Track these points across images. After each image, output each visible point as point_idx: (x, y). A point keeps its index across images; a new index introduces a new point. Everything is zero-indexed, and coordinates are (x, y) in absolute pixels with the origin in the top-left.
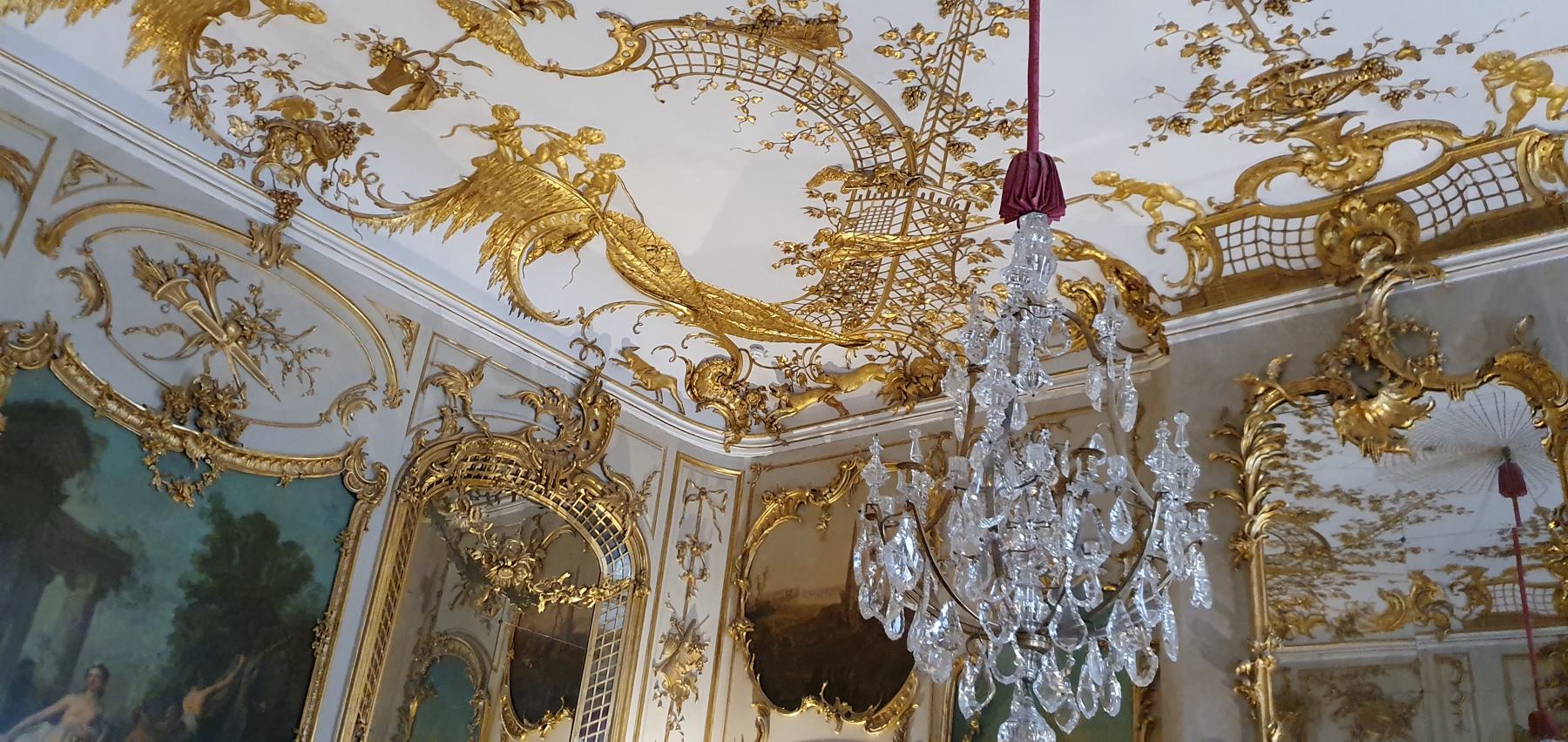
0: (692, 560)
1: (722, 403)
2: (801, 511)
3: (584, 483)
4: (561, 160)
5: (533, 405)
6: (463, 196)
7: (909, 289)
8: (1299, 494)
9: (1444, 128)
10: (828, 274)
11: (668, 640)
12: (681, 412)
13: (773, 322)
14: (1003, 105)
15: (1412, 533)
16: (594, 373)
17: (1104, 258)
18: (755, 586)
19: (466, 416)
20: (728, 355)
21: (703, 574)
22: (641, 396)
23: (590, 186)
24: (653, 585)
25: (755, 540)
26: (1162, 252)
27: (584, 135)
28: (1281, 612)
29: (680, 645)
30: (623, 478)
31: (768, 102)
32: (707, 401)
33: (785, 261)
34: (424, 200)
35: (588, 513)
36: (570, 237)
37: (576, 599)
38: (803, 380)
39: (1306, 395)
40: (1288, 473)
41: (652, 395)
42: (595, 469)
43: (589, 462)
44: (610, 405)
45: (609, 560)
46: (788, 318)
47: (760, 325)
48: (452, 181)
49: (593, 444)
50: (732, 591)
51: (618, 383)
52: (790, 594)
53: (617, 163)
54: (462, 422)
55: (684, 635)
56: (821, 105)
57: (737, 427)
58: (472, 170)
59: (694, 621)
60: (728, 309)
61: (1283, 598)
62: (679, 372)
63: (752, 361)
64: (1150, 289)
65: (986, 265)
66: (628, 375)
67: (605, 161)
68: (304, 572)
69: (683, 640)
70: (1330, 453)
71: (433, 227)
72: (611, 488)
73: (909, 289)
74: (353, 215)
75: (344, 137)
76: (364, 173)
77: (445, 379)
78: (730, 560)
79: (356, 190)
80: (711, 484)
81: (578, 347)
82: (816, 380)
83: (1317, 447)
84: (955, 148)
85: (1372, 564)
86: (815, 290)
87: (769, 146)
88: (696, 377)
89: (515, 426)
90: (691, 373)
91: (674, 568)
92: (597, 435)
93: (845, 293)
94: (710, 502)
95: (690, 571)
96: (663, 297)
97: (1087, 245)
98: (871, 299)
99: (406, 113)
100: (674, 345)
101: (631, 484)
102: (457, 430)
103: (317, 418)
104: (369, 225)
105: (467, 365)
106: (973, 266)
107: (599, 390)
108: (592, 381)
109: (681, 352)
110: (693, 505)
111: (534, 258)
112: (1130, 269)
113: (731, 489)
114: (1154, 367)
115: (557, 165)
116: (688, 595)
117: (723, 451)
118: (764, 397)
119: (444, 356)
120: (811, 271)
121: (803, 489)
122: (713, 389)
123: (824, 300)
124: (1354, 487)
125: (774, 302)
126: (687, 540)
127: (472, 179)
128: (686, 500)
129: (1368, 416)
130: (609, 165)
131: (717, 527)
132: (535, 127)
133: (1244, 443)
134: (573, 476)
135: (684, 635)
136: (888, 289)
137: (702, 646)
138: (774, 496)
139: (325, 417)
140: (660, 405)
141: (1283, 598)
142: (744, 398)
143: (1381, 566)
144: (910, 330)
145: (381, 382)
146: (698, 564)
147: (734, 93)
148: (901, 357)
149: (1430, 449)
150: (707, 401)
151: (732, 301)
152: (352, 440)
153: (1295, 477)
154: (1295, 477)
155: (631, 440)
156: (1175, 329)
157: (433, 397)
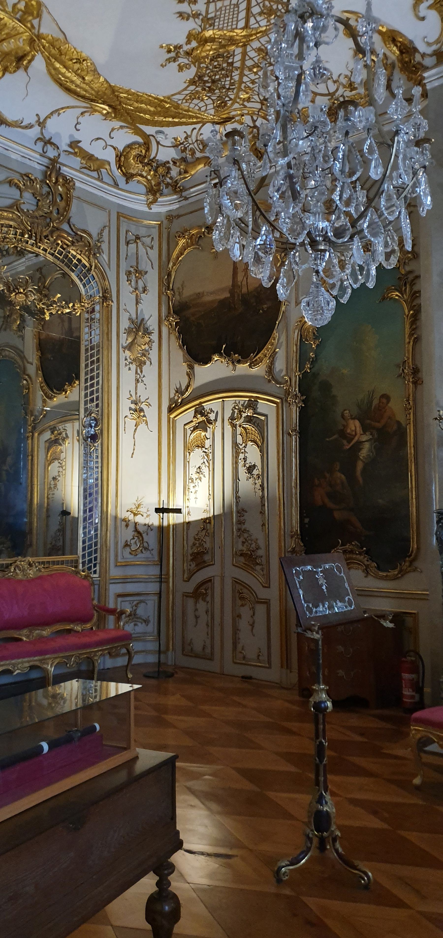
0: (137, 282)
1: (142, 176)
2: (200, 242)
3: (59, 237)
7: (256, 73)
10: (199, 67)
11: (129, 331)
12: (116, 185)
13: (167, 111)
18: (177, 293)
20: (140, 140)
21: (145, 290)
22: (88, 175)
24: (114, 299)
25: (174, 264)
29: (136, 334)
30: (84, 231)
32: (132, 176)
33: (169, 60)
35: (66, 256)
37: (68, 311)
38: (193, 153)
41: (95, 174)
42: (65, 226)
43: (61, 222)
44: (68, 182)
45: (84, 285)
46: (177, 107)
47: (159, 114)
49: (61, 210)
50: (164, 298)
51: (71, 167)
52: (199, 295)
55: (138, 327)
57: (154, 192)
59: (143, 320)
60: (136, 105)
62: (110, 156)
63: (158, 143)
66: (77, 161)
69: (138, 330)
72: (78, 239)
73: (256, 73)
78: (160, 279)
80: (142, 232)
82: (202, 151)
86: (192, 82)
88: (123, 159)
90: (119, 157)
91: (126, 288)
92: (62, 204)
93: (213, 82)
94: (143, 244)
95: (136, 289)
96: (90, 99)
98: (232, 84)
100: (103, 135)
101: (90, 235)
107: (59, 174)
108: (54, 166)
109: (110, 142)
110: (133, 246)
113: (155, 233)
116: (137, 303)
117: (146, 209)
118: (169, 169)
120: (187, 66)
121: (200, 227)
122: (135, 167)
123: (199, 89)
125: (166, 94)
126: (132, 270)
128: (128, 243)
131: (149, 259)
134: (52, 232)
135: (138, 327)
136: (242, 75)
137: (150, 333)
138: (182, 234)
140: (100, 179)
142: (156, 171)
144: (259, 106)
146: (141, 284)
148: (255, 127)
150: (132, 176)
151: (138, 98)
155: (84, 205)
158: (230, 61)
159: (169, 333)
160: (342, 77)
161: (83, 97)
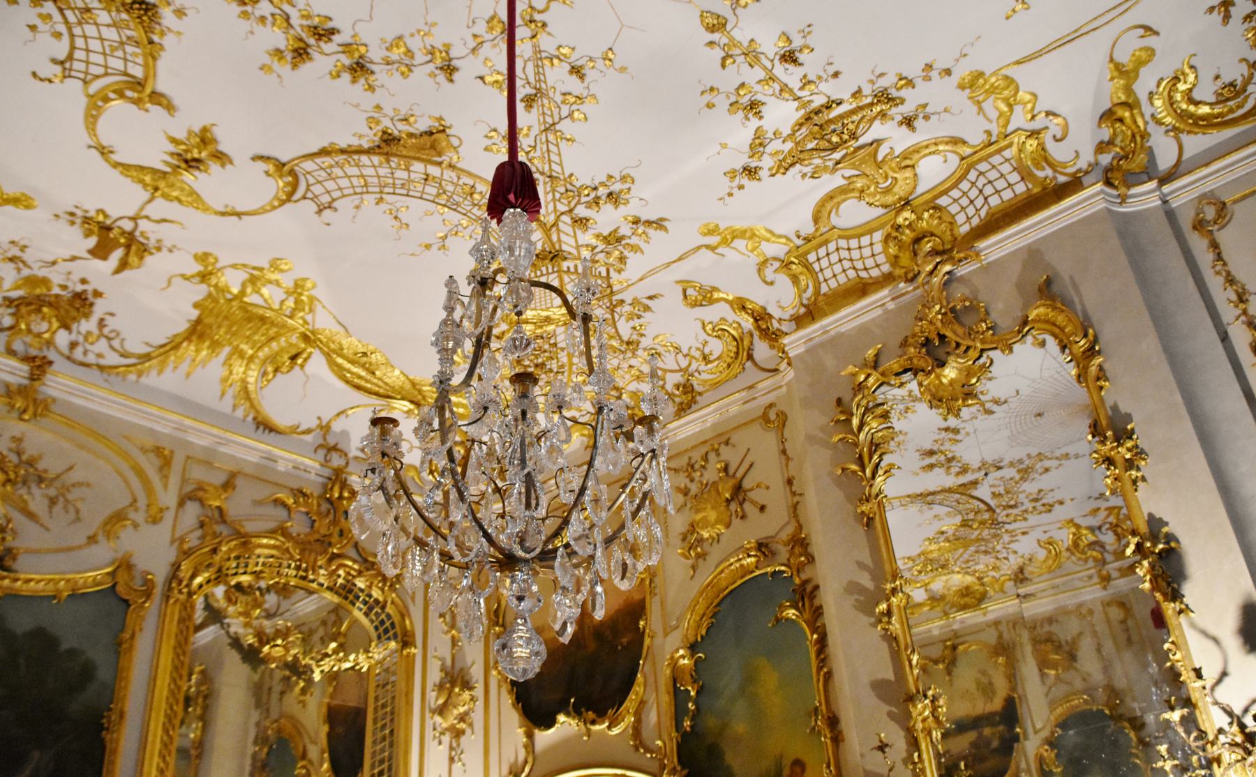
4: (265, 291)
5: (284, 505)
6: (194, 338)
8: (958, 474)
9: (956, 141)
14: (604, 179)
15: (1044, 482)
16: (338, 472)
17: (731, 298)
19: (224, 522)
23: (294, 310)
26: (772, 283)
27: (275, 265)
28: (980, 579)
31: (413, 209)
34: (164, 345)
36: (294, 358)
39: (898, 374)
40: (942, 458)
48: (183, 327)
53: (309, 285)
54: (219, 528)
55: (456, 679)
56: (457, 204)
58: (195, 314)
61: (977, 567)
64: (770, 316)
65: (641, 321)
67: (299, 286)
68: (87, 672)
70: (968, 434)
71: (176, 368)
74: (101, 368)
75: (81, 303)
76: (106, 331)
77: (200, 494)
79: (102, 346)
81: (321, 453)
83: (956, 431)
84: (581, 222)
85: (1025, 519)
87: (428, 247)
89: (272, 525)
97: (715, 289)
99: (126, 274)
102: (215, 535)
103: (83, 540)
104: (118, 374)
105: (219, 479)
106: (631, 324)
111: (268, 381)
112: (752, 302)
114: (787, 379)
115: (262, 296)
119: (197, 473)
124: (996, 457)
127: (198, 321)
129: (945, 381)
130: (302, 287)
132: (234, 266)
133: (855, 422)
134: (330, 560)
139: (92, 539)
141: (977, 567)
143: (1033, 519)
145: (142, 503)
147: (383, 206)
149: (1039, 415)
152: (119, 555)
153: (950, 460)
154: (950, 460)
156: (795, 342)
157: (192, 512)
158: (552, 341)
159: (500, 687)
160: (693, 350)
161: (376, 394)
